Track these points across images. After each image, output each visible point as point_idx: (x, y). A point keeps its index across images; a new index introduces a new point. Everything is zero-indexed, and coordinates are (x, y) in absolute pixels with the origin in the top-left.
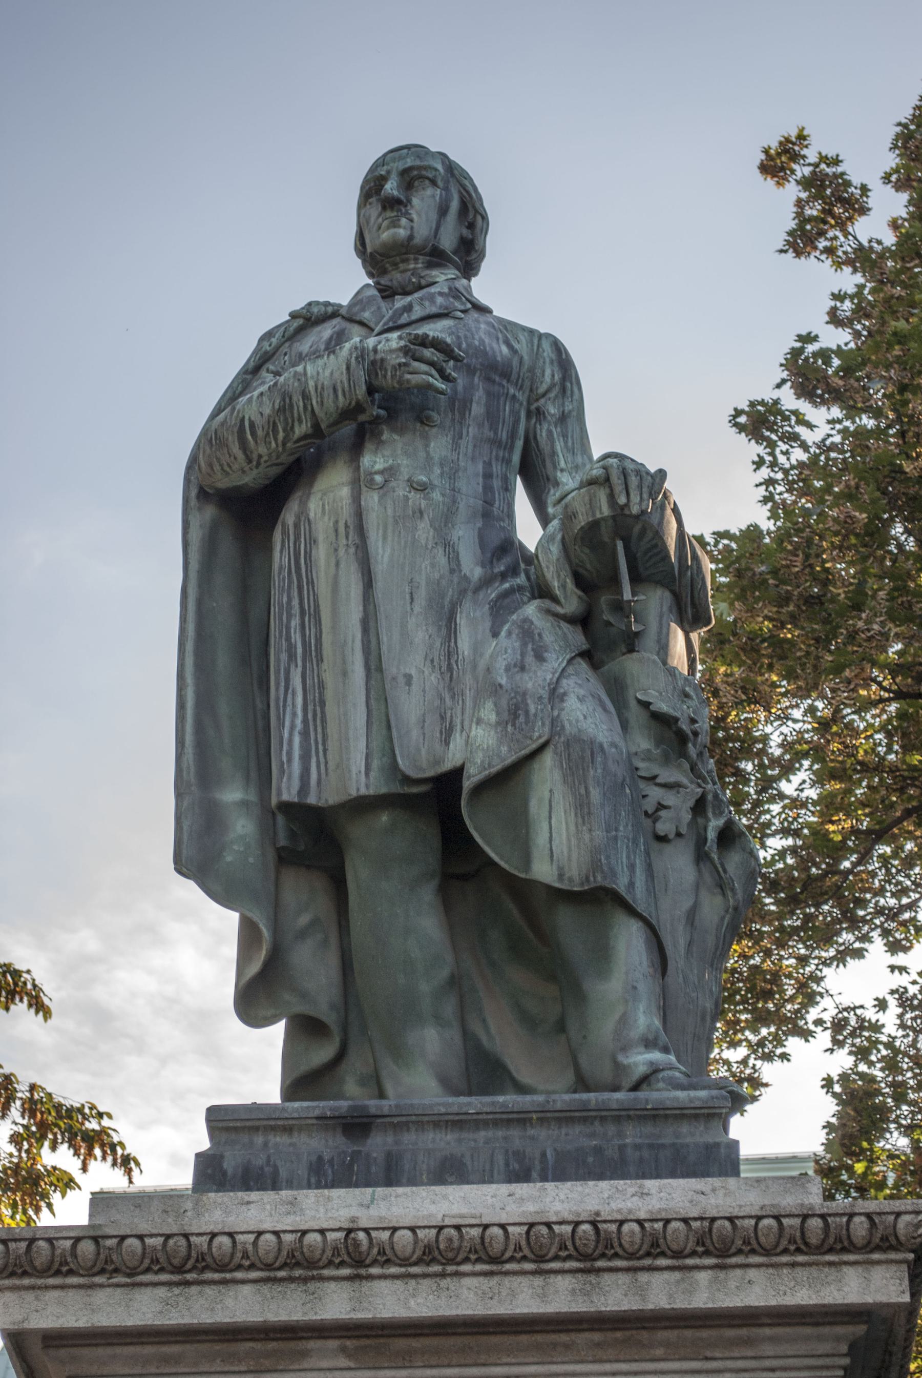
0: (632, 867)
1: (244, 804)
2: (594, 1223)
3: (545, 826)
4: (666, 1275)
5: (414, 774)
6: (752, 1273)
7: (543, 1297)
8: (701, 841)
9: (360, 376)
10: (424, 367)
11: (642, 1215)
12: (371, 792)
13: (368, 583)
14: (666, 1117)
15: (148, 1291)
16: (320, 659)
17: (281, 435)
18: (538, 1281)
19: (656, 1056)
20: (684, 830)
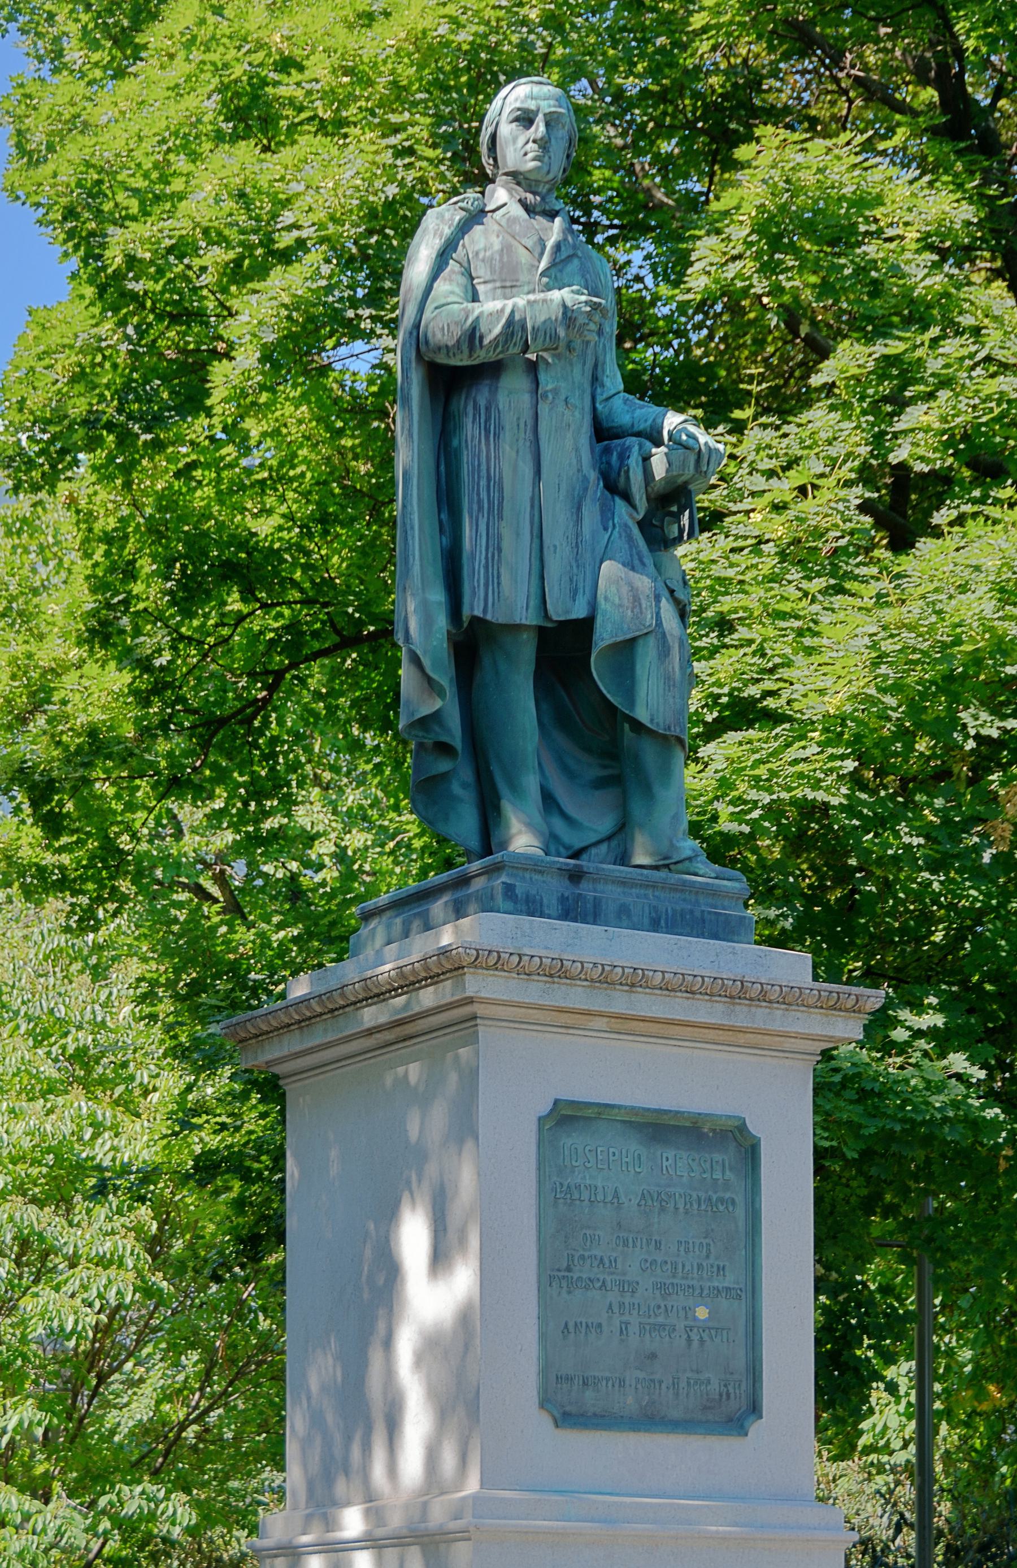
16: (501, 517)
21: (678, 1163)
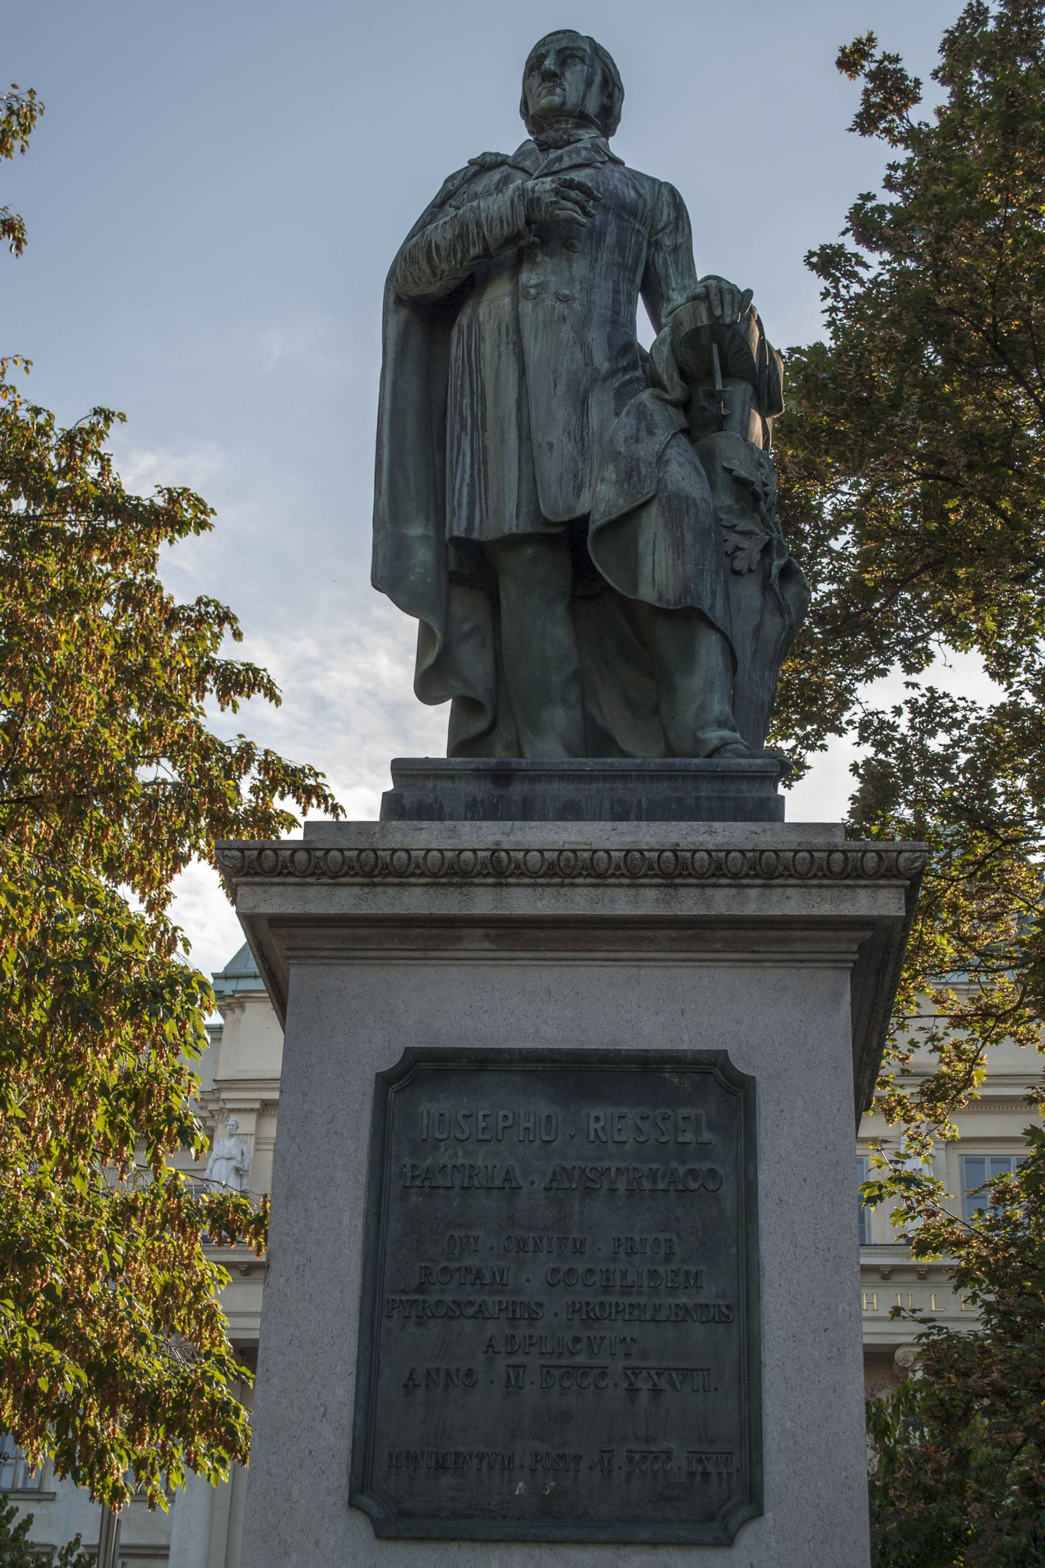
0: (714, 593)
1: (425, 537)
2: (674, 851)
3: (650, 561)
4: (726, 891)
5: (552, 518)
6: (790, 891)
7: (635, 904)
8: (767, 575)
9: (521, 210)
10: (570, 205)
11: (710, 847)
12: (520, 531)
13: (522, 372)
14: (731, 777)
15: (346, 889)
16: (484, 430)
17: (459, 255)
18: (632, 892)
19: (726, 733)
20: (754, 567)
21: (613, 1124)
